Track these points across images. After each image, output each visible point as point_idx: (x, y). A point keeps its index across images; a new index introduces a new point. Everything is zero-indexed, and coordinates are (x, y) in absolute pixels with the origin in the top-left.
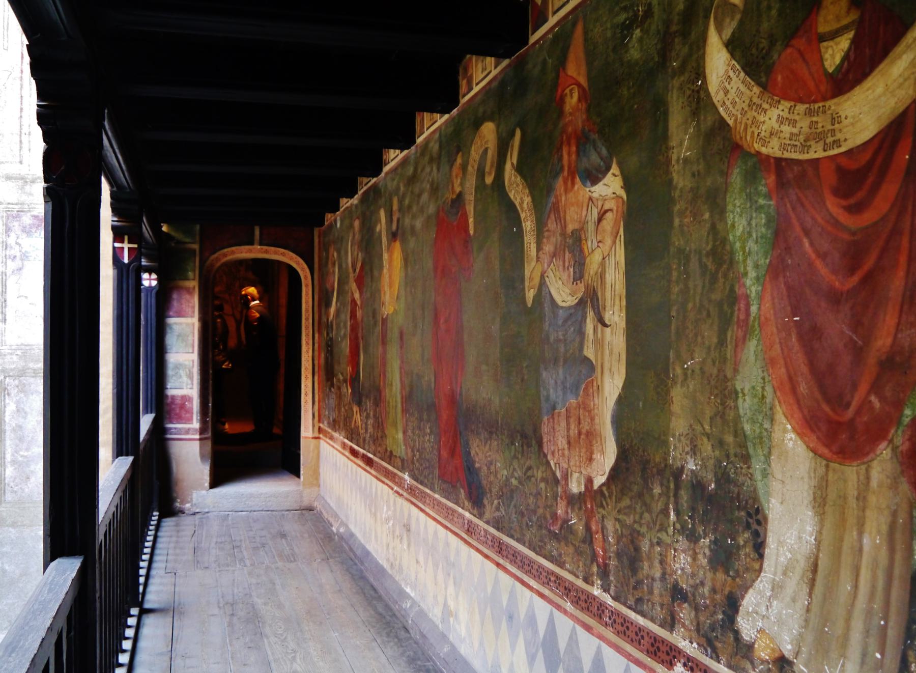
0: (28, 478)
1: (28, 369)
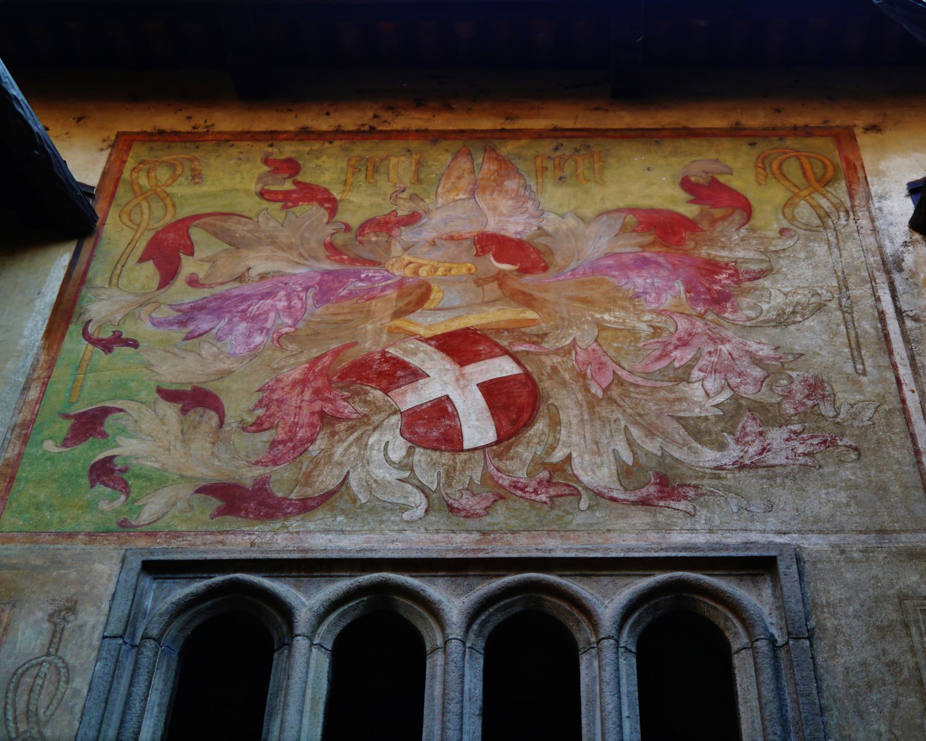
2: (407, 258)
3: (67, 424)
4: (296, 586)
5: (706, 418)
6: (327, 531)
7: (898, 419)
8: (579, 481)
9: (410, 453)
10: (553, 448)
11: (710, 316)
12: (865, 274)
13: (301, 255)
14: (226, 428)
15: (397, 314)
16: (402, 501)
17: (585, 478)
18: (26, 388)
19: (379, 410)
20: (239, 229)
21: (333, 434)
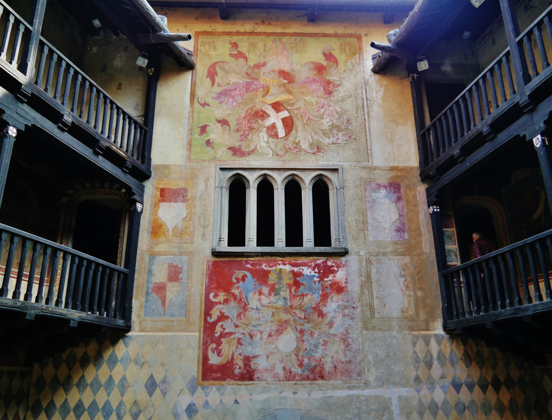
0: (385, 306)
2: (264, 78)
3: (199, 129)
4: (249, 173)
5: (326, 130)
6: (254, 160)
7: (364, 130)
8: (302, 147)
9: (268, 139)
10: (296, 138)
11: (328, 99)
12: (360, 85)
13: (241, 76)
14: (231, 131)
15: (264, 96)
16: (268, 152)
17: (303, 147)
18: (189, 119)
19: (261, 126)
20: (227, 67)
21: (253, 133)
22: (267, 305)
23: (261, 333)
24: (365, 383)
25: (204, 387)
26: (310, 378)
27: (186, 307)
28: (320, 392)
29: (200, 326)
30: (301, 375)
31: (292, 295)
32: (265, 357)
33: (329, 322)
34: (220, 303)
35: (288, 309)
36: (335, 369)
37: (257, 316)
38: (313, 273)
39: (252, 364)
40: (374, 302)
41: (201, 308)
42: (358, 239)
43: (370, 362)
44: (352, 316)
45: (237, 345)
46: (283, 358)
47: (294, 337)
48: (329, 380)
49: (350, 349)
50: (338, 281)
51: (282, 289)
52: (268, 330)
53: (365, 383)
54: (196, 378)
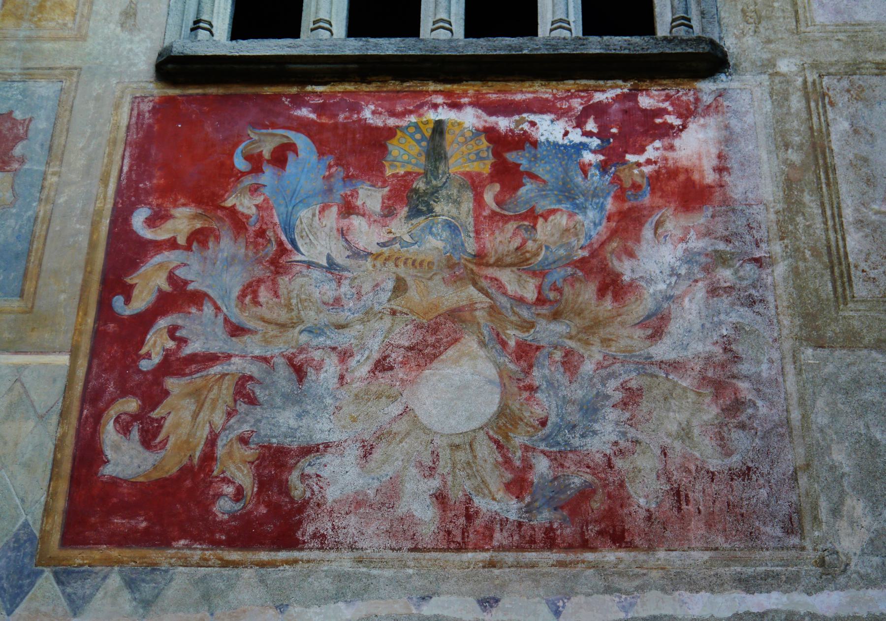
1: (866, 62)
22: (375, 249)
23: (344, 355)
24: (822, 563)
25: (69, 573)
26: (559, 541)
27: (28, 261)
28: (607, 597)
29: (78, 332)
30: (520, 525)
31: (486, 213)
32: (353, 453)
33: (648, 317)
34: (172, 244)
35: (466, 267)
36: (679, 501)
37: (329, 290)
38: (576, 136)
39: (294, 477)
40: (848, 239)
41: (89, 262)
42: (769, 18)
43: (843, 475)
44: (753, 292)
45: (231, 404)
46: (435, 455)
47: (492, 372)
48: (651, 549)
49: (747, 422)
50: (685, 163)
51: (444, 192)
52: (375, 347)
53: (822, 563)
54: (38, 535)
